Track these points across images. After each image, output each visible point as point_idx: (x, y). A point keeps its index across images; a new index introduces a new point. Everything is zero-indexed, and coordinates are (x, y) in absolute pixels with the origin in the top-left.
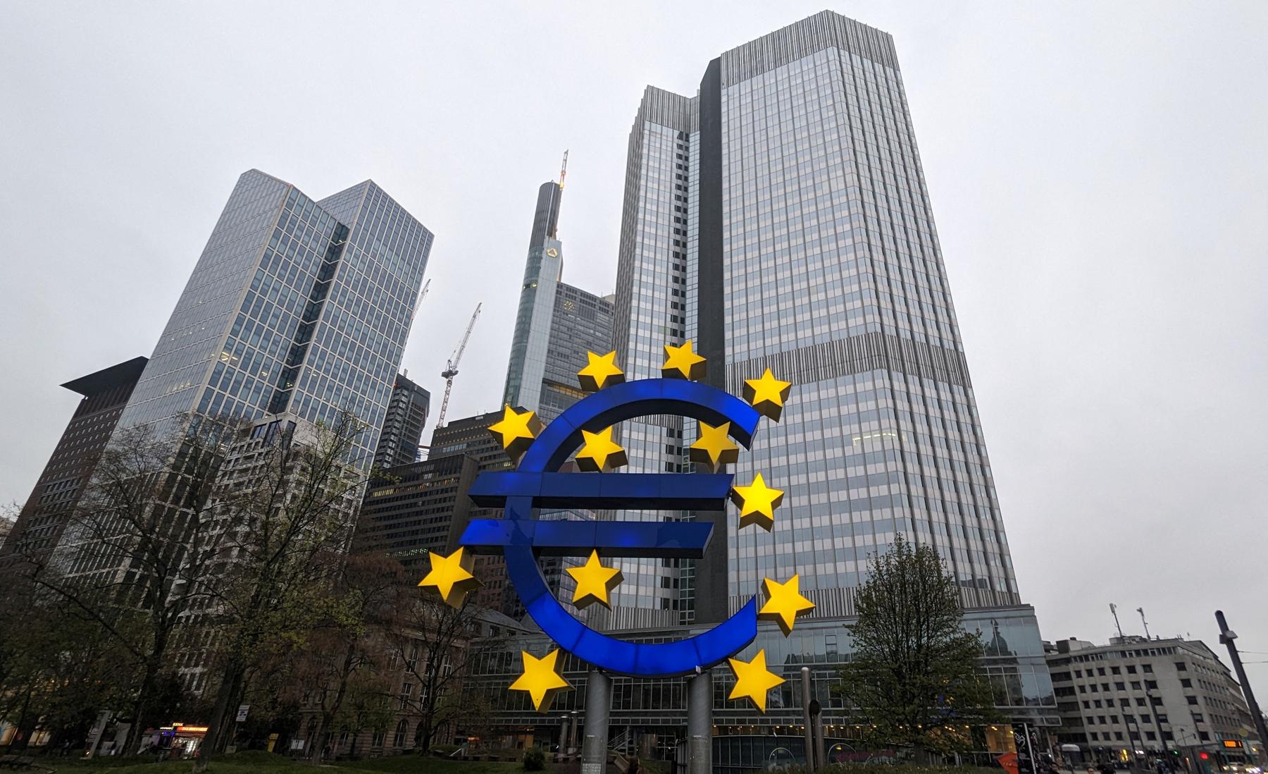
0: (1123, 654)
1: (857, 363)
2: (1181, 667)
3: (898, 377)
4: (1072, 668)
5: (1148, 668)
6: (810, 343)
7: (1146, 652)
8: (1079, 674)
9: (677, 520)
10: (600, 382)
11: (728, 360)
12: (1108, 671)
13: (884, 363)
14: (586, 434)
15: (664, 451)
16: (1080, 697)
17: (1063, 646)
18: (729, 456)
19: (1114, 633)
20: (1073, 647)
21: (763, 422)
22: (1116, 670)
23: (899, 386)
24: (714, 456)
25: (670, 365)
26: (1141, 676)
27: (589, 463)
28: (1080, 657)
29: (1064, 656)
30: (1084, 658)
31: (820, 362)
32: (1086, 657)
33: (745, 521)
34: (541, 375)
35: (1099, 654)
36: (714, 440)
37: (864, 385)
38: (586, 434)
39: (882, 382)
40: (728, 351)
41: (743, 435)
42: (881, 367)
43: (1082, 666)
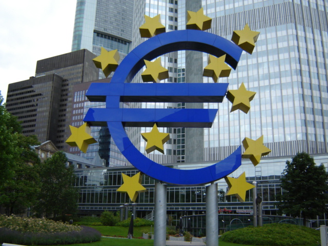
1: (278, 20)
3: (300, 27)
6: (252, 8)
10: (152, 32)
13: (293, 20)
14: (146, 61)
18: (225, 73)
21: (244, 52)
23: (301, 33)
24: (218, 73)
25: (191, 22)
27: (147, 78)
31: (257, 19)
33: (234, 109)
34: (92, 28)
37: (282, 33)
38: (146, 61)
39: (292, 31)
41: (233, 62)
42: (291, 22)
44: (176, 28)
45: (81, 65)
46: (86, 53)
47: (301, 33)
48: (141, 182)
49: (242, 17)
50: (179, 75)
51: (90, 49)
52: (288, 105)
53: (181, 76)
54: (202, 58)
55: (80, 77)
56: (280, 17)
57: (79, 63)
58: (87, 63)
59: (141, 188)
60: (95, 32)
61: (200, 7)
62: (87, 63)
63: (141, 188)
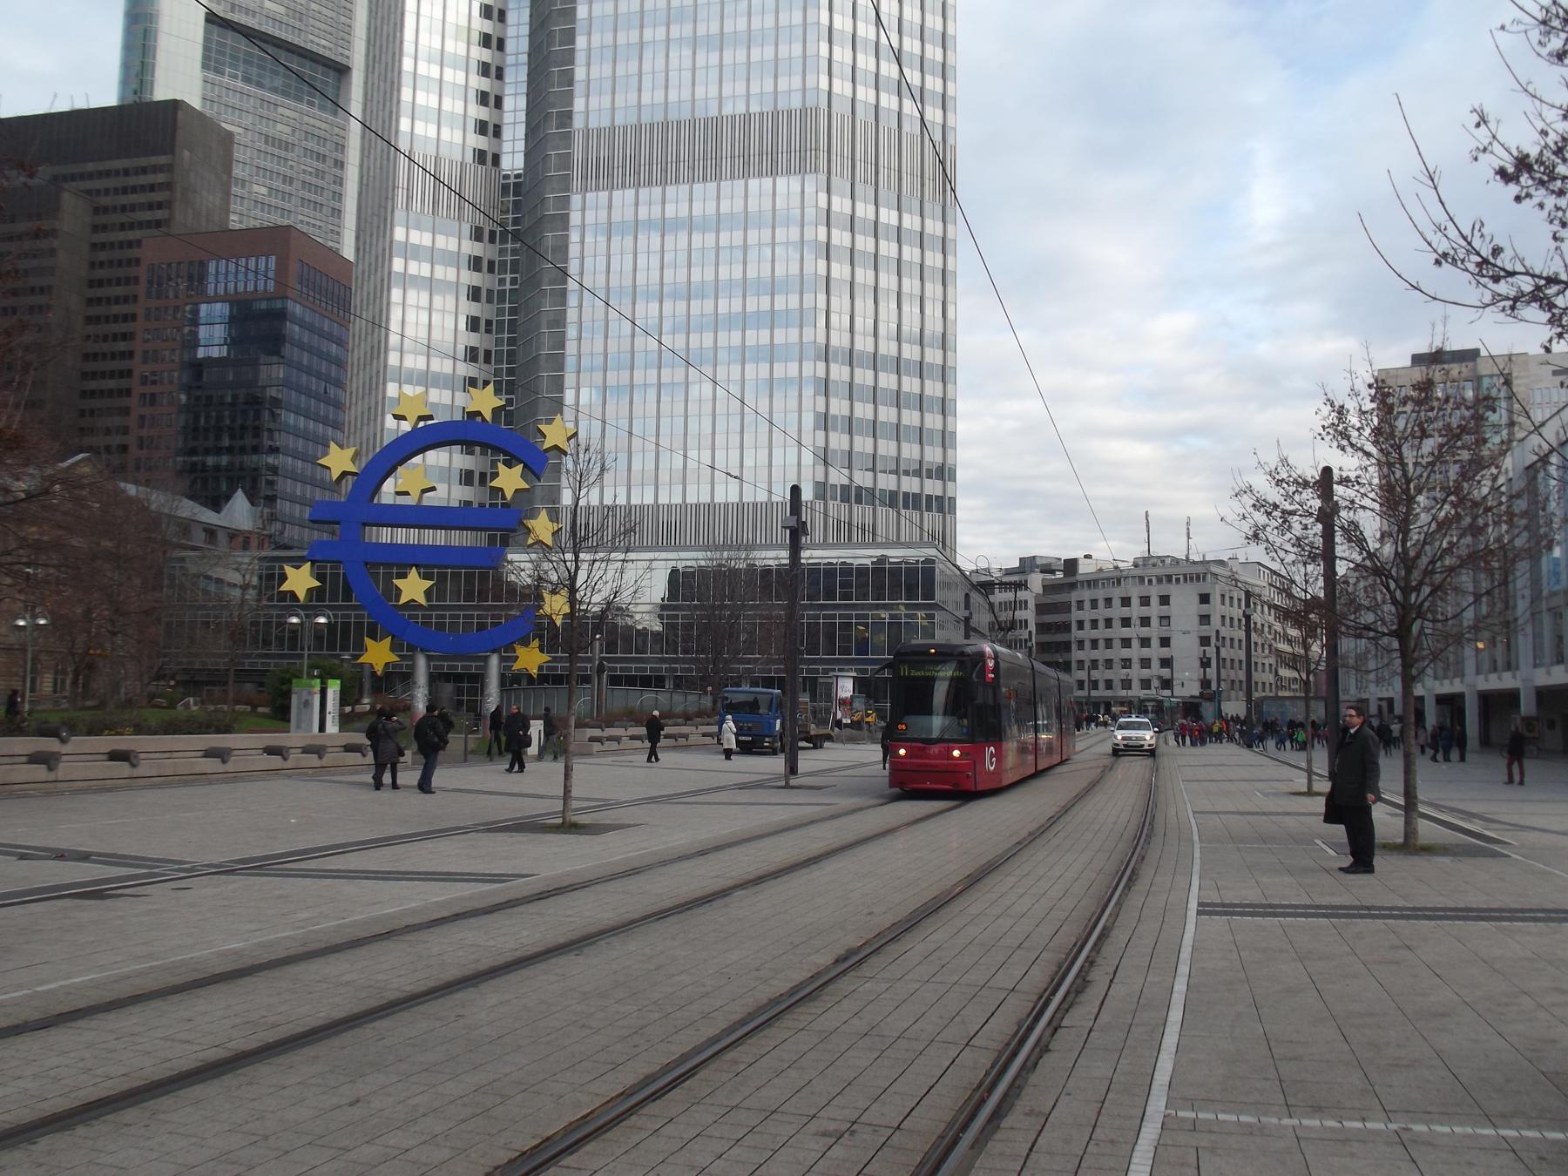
0: (1142, 579)
1: (782, 159)
2: (1205, 599)
3: (841, 183)
4: (1074, 596)
5: (1165, 600)
7: (1169, 578)
8: (1080, 605)
9: (482, 505)
11: (578, 122)
12: (1116, 602)
15: (462, 325)
16: (1076, 634)
17: (1071, 565)
19: (1139, 551)
20: (1085, 568)
22: (1126, 602)
23: (841, 205)
26: (1155, 610)
28: (1089, 582)
29: (1070, 580)
30: (1092, 583)
32: (1096, 582)
35: (1117, 578)
36: (510, 480)
40: (579, 104)
43: (1086, 595)
44: (496, 159)
45: (162, 160)
46: (180, 114)
47: (841, 205)
48: (393, 649)
49: (685, 134)
50: (502, 282)
51: (196, 103)
52: (784, 403)
53: (508, 286)
54: (567, 247)
55: (160, 205)
56: (789, 152)
57: (154, 153)
58: (186, 154)
59: (393, 658)
60: (212, 18)
61: (571, 82)
62: (186, 154)
63: (393, 658)
